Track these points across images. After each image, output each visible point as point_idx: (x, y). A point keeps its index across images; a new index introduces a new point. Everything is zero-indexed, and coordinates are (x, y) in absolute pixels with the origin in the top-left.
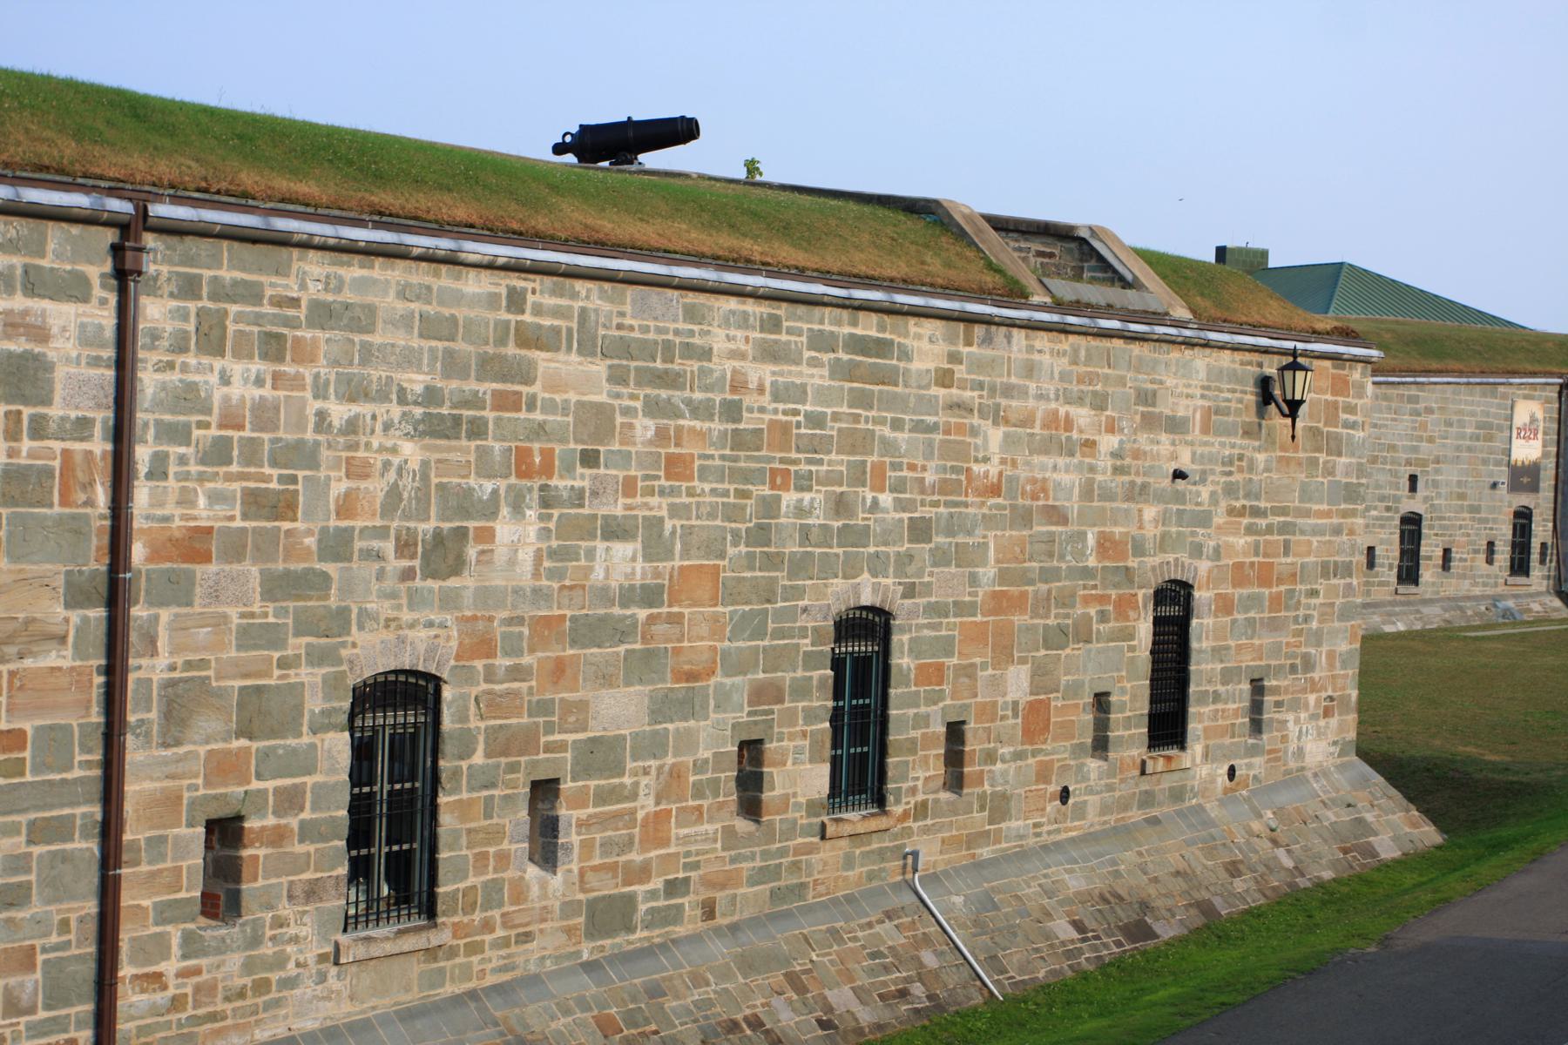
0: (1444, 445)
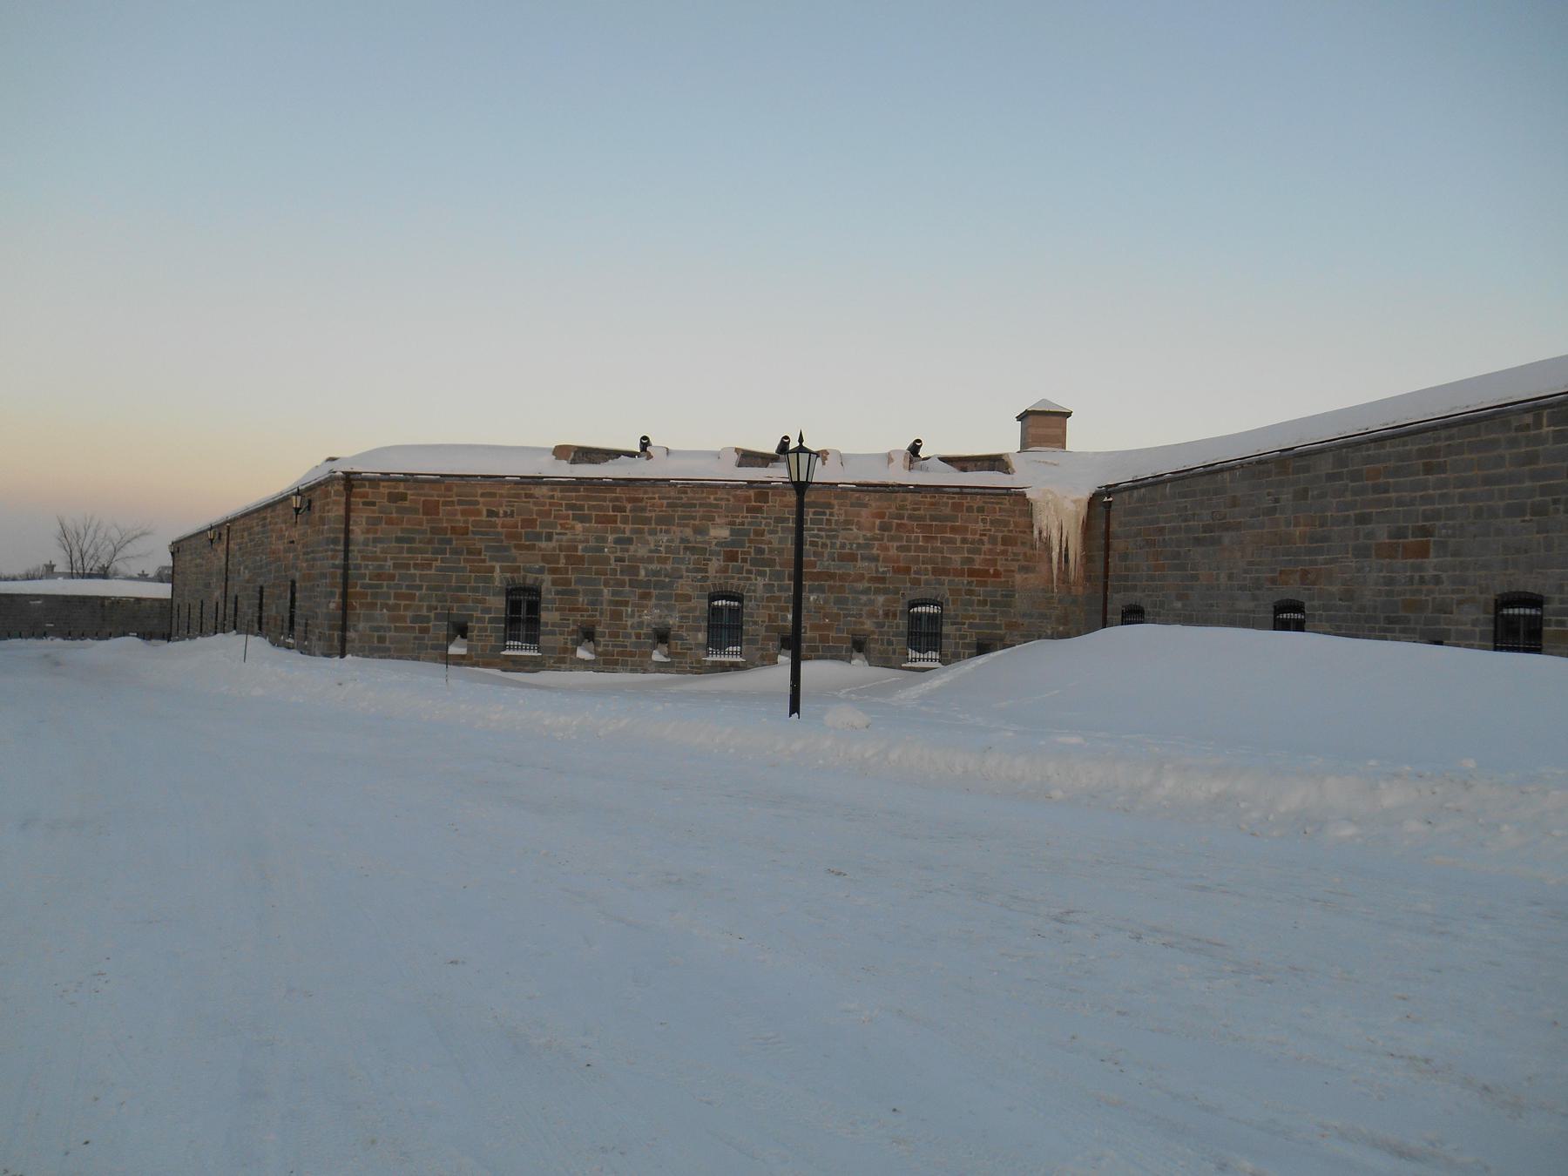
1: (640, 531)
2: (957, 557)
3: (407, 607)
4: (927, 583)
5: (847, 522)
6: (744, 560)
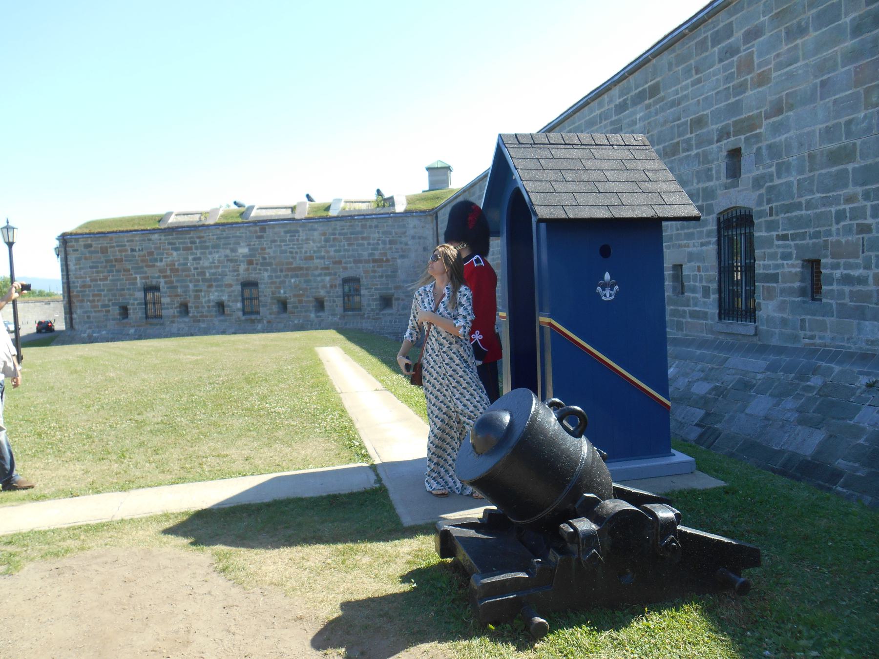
0: (790, 76)
1: (204, 253)
2: (366, 254)
3: (98, 301)
4: (351, 268)
5: (307, 239)
6: (257, 264)
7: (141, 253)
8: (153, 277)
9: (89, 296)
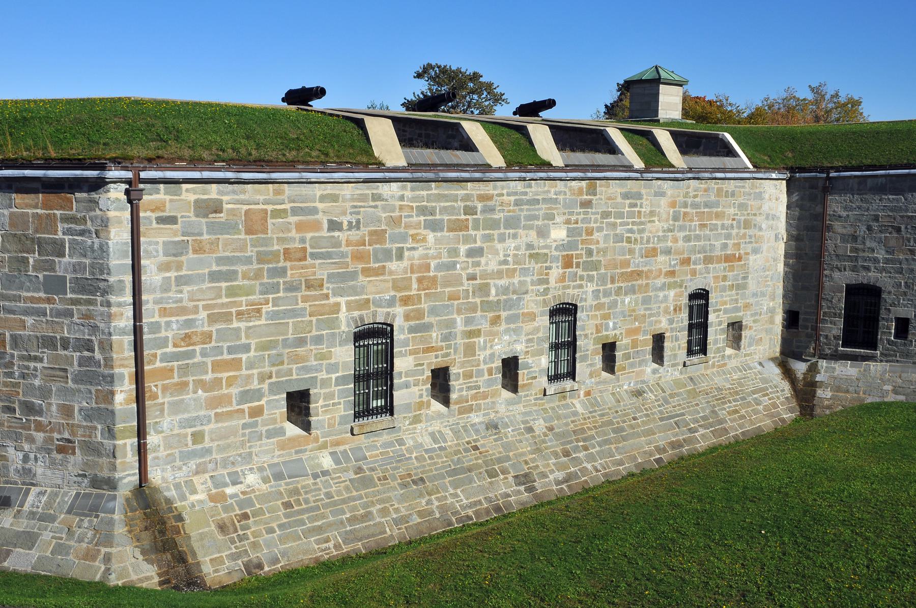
3: (231, 382)
7: (354, 235)
8: (378, 303)
9: (201, 367)
